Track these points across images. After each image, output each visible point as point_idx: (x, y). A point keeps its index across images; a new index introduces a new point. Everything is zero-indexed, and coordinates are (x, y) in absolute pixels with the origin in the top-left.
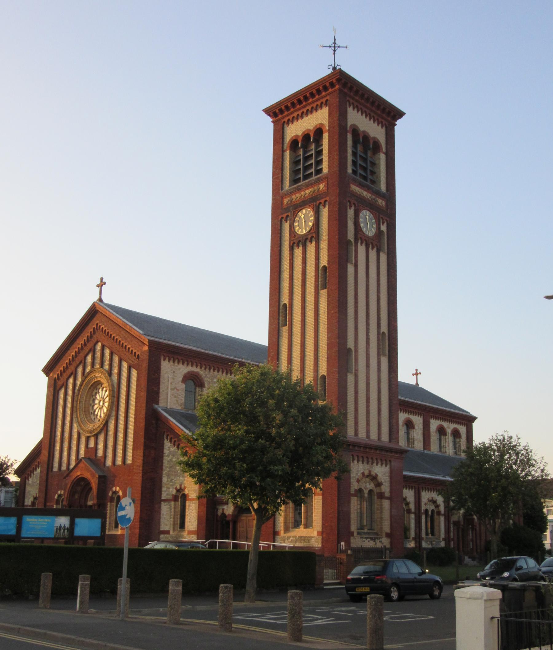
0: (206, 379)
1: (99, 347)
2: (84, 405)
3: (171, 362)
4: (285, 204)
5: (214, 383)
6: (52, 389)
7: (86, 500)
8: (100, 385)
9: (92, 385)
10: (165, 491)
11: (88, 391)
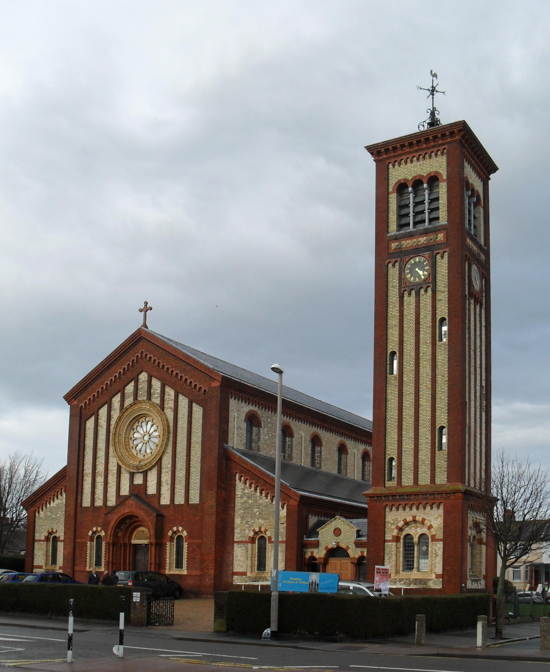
0: (262, 419)
1: (143, 377)
2: (123, 438)
3: (237, 401)
4: (393, 248)
5: (269, 423)
6: (78, 418)
7: (130, 538)
8: (144, 418)
9: (134, 418)
10: (238, 533)
11: (129, 424)
